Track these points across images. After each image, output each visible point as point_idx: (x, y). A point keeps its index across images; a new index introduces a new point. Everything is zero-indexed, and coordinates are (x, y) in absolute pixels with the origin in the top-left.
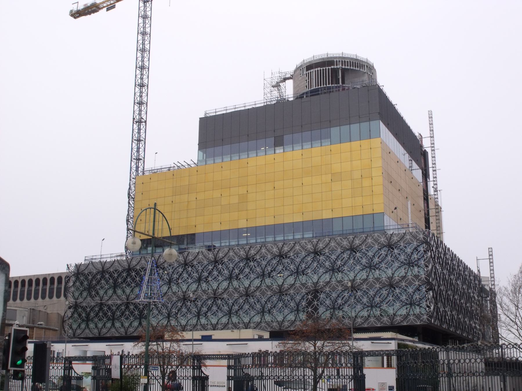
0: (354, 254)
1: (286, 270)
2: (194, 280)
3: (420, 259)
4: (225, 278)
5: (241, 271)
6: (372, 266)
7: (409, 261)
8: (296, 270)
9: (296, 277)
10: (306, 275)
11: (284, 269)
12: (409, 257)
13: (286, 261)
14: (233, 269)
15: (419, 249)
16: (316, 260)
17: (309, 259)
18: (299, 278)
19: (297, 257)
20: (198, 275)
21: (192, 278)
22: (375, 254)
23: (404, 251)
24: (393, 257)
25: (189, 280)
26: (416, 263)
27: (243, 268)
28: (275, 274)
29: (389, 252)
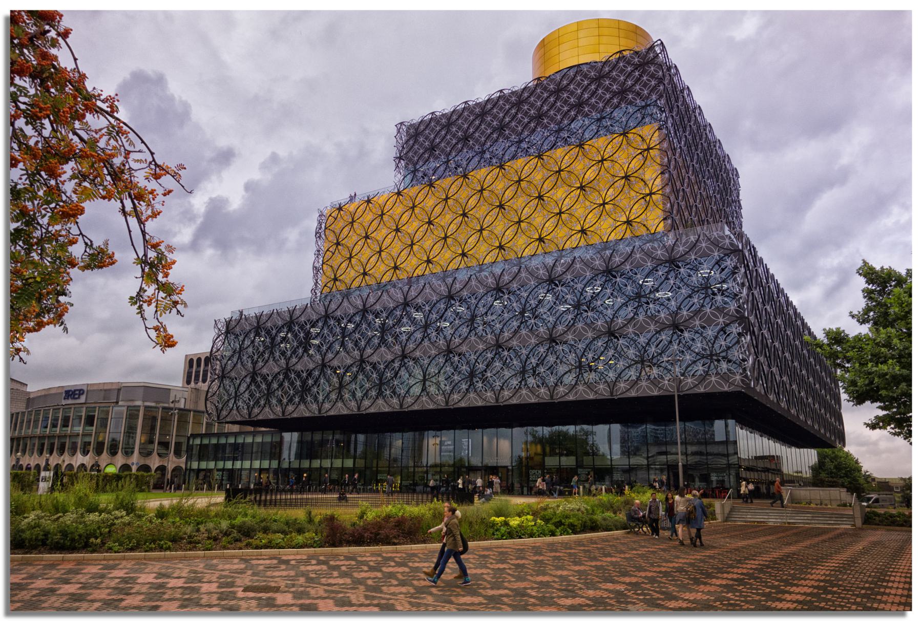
0: (616, 340)
1: (561, 363)
2: (463, 377)
3: (731, 347)
4: (513, 373)
5: (541, 362)
6: (645, 361)
7: (711, 352)
8: (577, 364)
9: (578, 376)
10: (595, 371)
11: (558, 361)
12: (710, 345)
13: (561, 348)
14: (528, 357)
15: (728, 330)
16: (611, 345)
17: (600, 344)
18: (582, 376)
19: (580, 341)
20: (470, 368)
21: (460, 373)
22: (650, 340)
23: (701, 334)
24: (681, 345)
25: (456, 377)
26: (724, 354)
27: (544, 355)
28: (542, 370)
29: (675, 337)
